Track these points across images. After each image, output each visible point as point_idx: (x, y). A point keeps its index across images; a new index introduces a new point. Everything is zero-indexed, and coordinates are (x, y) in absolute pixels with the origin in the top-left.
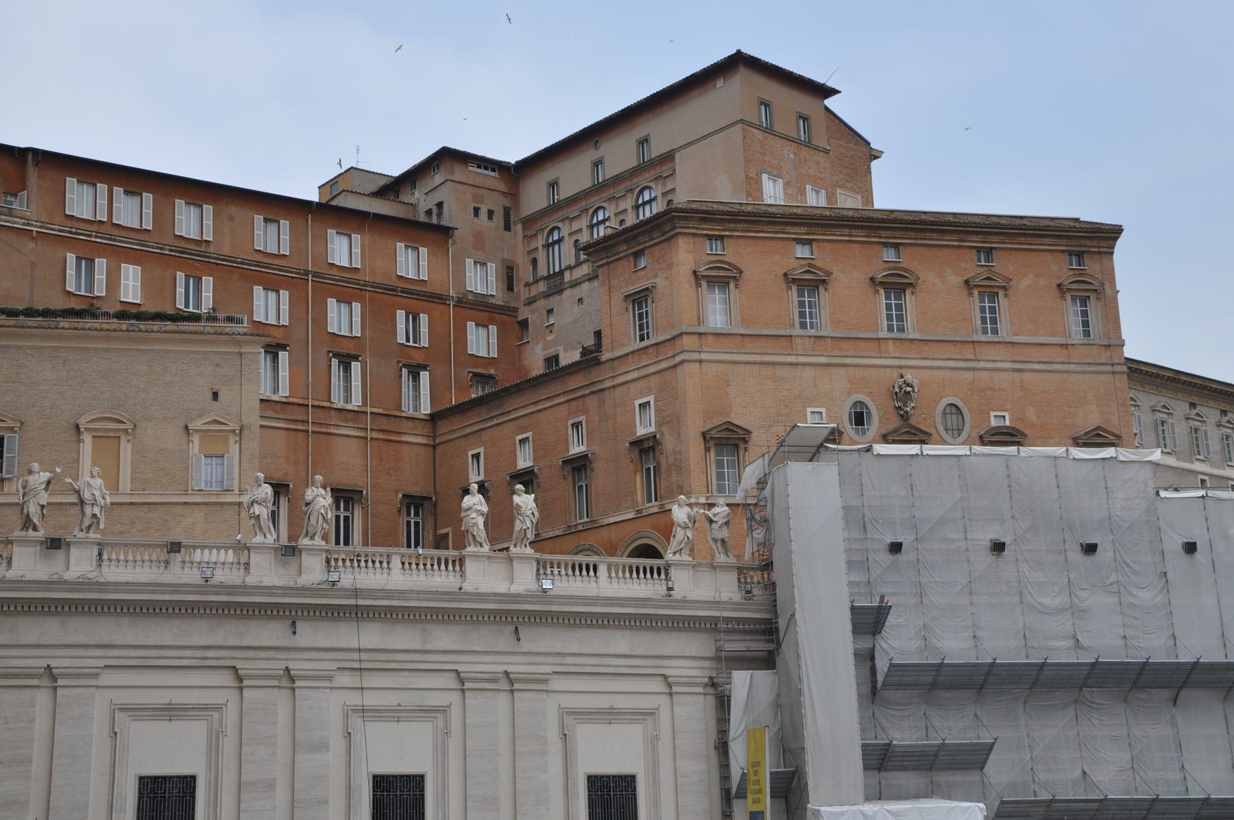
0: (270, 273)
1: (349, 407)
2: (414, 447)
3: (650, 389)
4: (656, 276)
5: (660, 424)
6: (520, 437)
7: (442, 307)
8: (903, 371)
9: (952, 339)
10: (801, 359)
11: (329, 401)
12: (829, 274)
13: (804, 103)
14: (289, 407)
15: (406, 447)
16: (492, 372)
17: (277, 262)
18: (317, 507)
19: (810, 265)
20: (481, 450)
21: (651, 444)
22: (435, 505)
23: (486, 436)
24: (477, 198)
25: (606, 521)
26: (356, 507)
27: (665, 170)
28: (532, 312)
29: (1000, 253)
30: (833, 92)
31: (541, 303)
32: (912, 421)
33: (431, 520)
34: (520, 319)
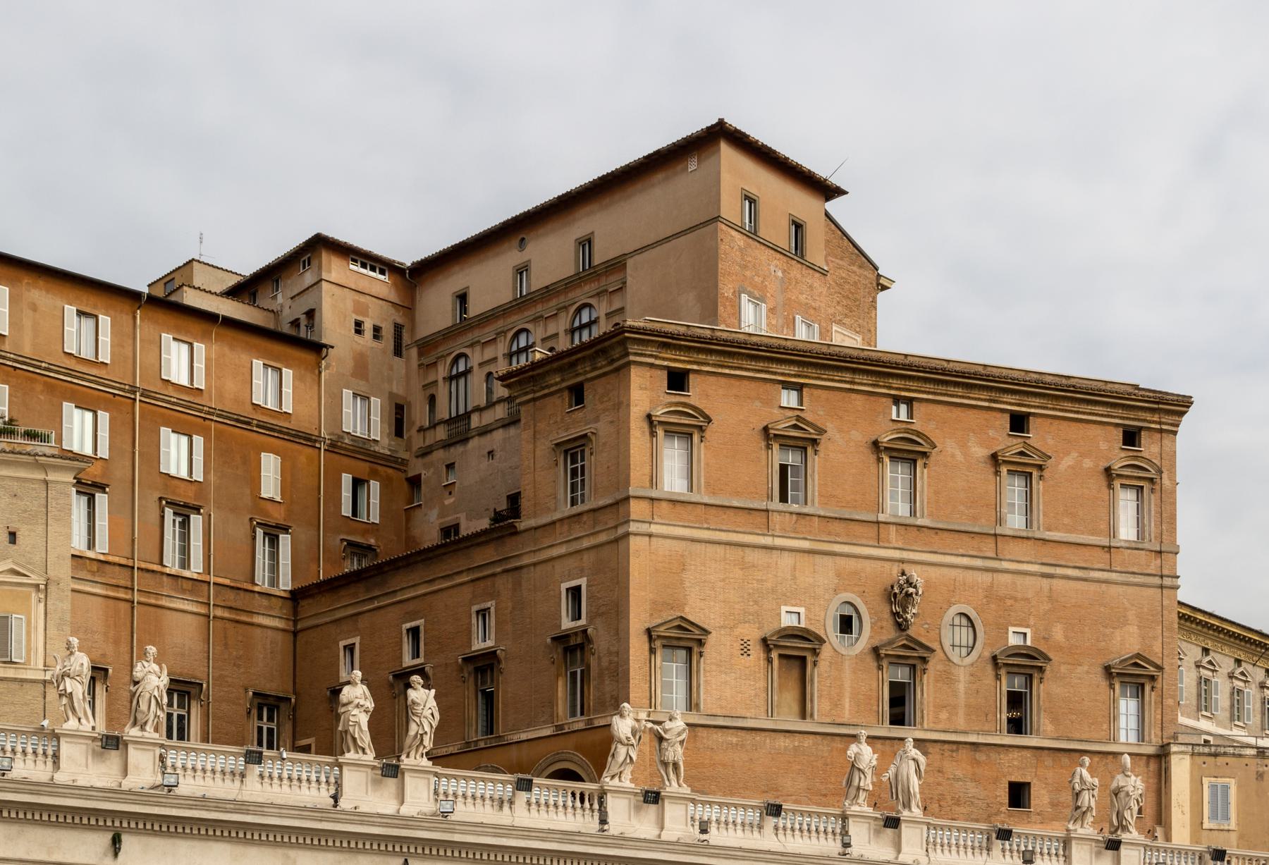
0: (86, 385)
1: (186, 574)
2: (270, 632)
3: (582, 570)
4: (597, 420)
6: (408, 625)
7: (310, 450)
8: (906, 567)
9: (970, 529)
10: (779, 542)
11: (161, 563)
12: (822, 431)
14: (107, 567)
15: (258, 631)
16: (372, 541)
17: (94, 371)
18: (149, 688)
19: (799, 418)
20: (357, 640)
21: (579, 640)
22: (294, 710)
23: (363, 622)
24: (360, 308)
25: (516, 738)
26: (193, 703)
27: (612, 282)
28: (426, 466)
29: (1039, 420)
31: (439, 455)
32: (911, 632)
33: (288, 727)
34: (411, 474)
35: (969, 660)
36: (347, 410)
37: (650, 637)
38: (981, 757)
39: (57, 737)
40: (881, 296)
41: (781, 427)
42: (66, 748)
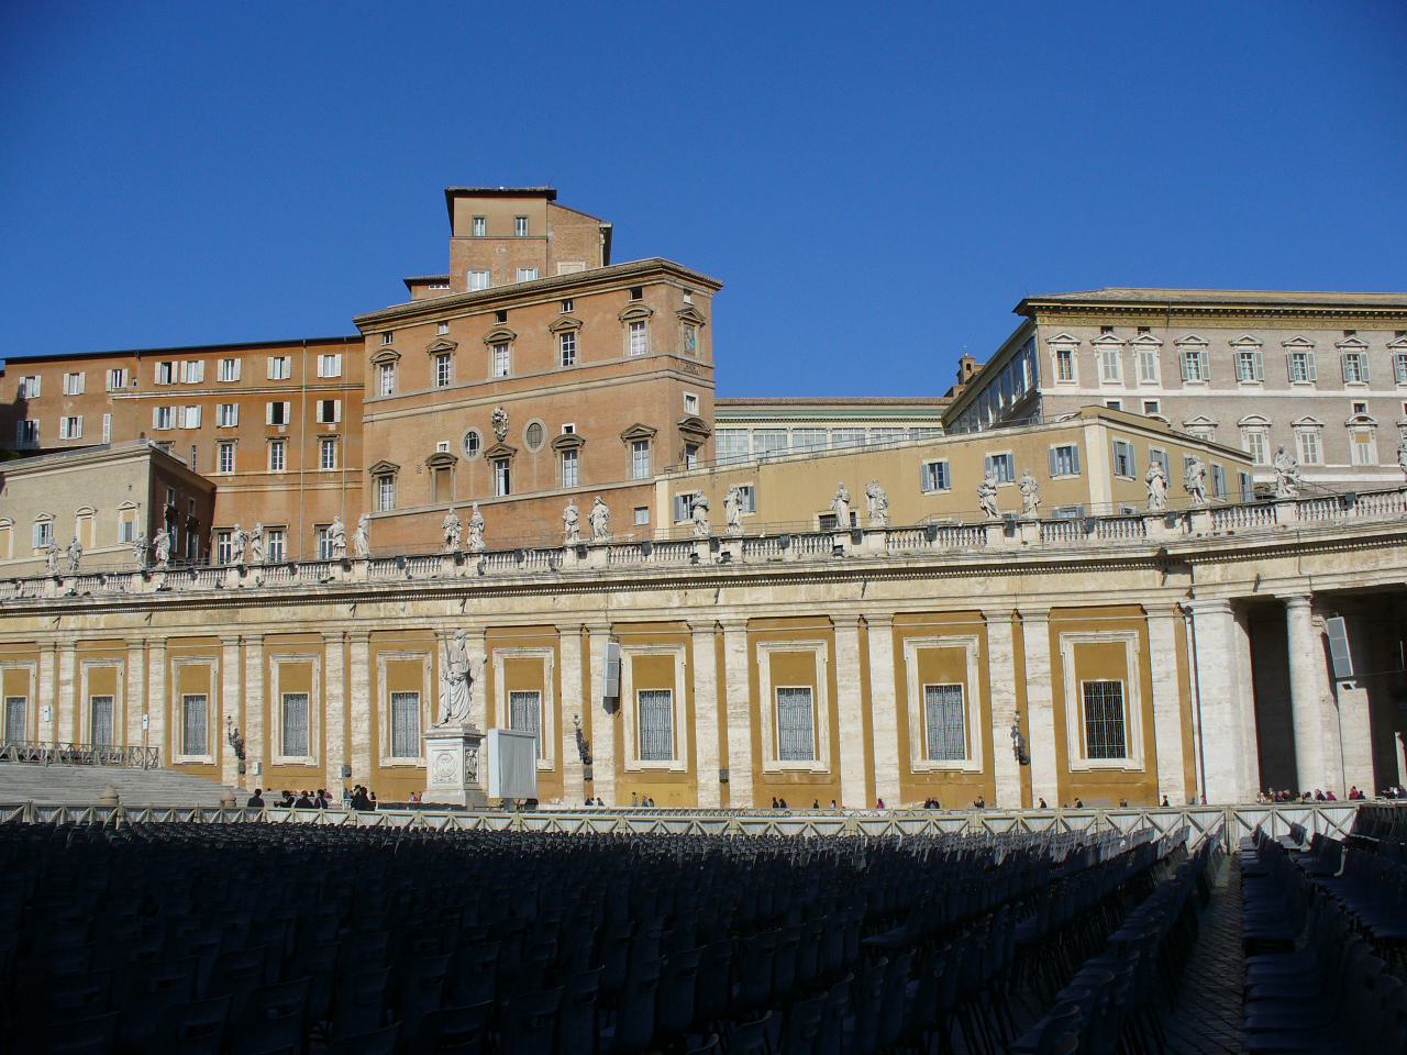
38: (547, 505)
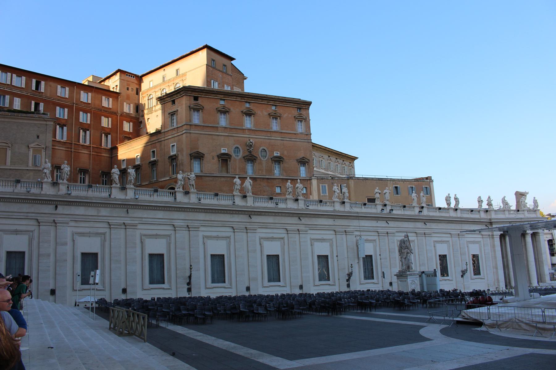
5: (177, 151)
10: (220, 134)
13: (225, 61)
24: (128, 85)
30: (233, 59)
35: (265, 159)
36: (125, 107)
37: (191, 157)
39: (42, 183)
40: (245, 81)
41: (220, 109)
42: (44, 186)
